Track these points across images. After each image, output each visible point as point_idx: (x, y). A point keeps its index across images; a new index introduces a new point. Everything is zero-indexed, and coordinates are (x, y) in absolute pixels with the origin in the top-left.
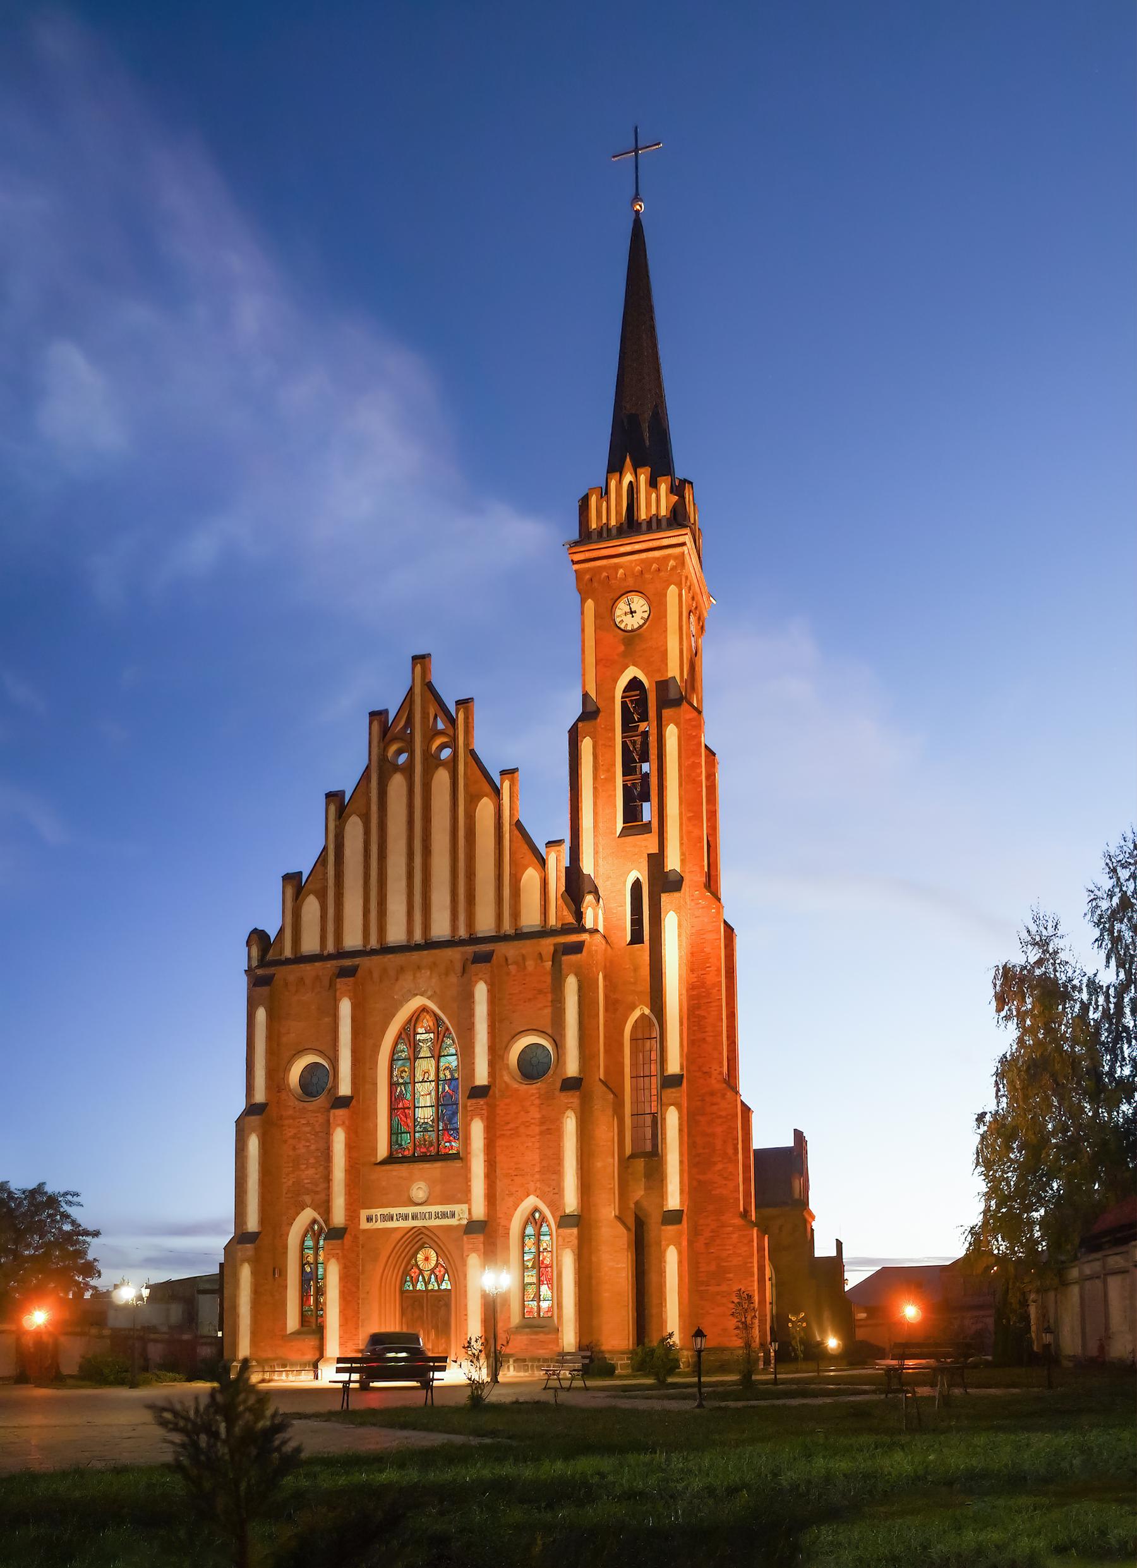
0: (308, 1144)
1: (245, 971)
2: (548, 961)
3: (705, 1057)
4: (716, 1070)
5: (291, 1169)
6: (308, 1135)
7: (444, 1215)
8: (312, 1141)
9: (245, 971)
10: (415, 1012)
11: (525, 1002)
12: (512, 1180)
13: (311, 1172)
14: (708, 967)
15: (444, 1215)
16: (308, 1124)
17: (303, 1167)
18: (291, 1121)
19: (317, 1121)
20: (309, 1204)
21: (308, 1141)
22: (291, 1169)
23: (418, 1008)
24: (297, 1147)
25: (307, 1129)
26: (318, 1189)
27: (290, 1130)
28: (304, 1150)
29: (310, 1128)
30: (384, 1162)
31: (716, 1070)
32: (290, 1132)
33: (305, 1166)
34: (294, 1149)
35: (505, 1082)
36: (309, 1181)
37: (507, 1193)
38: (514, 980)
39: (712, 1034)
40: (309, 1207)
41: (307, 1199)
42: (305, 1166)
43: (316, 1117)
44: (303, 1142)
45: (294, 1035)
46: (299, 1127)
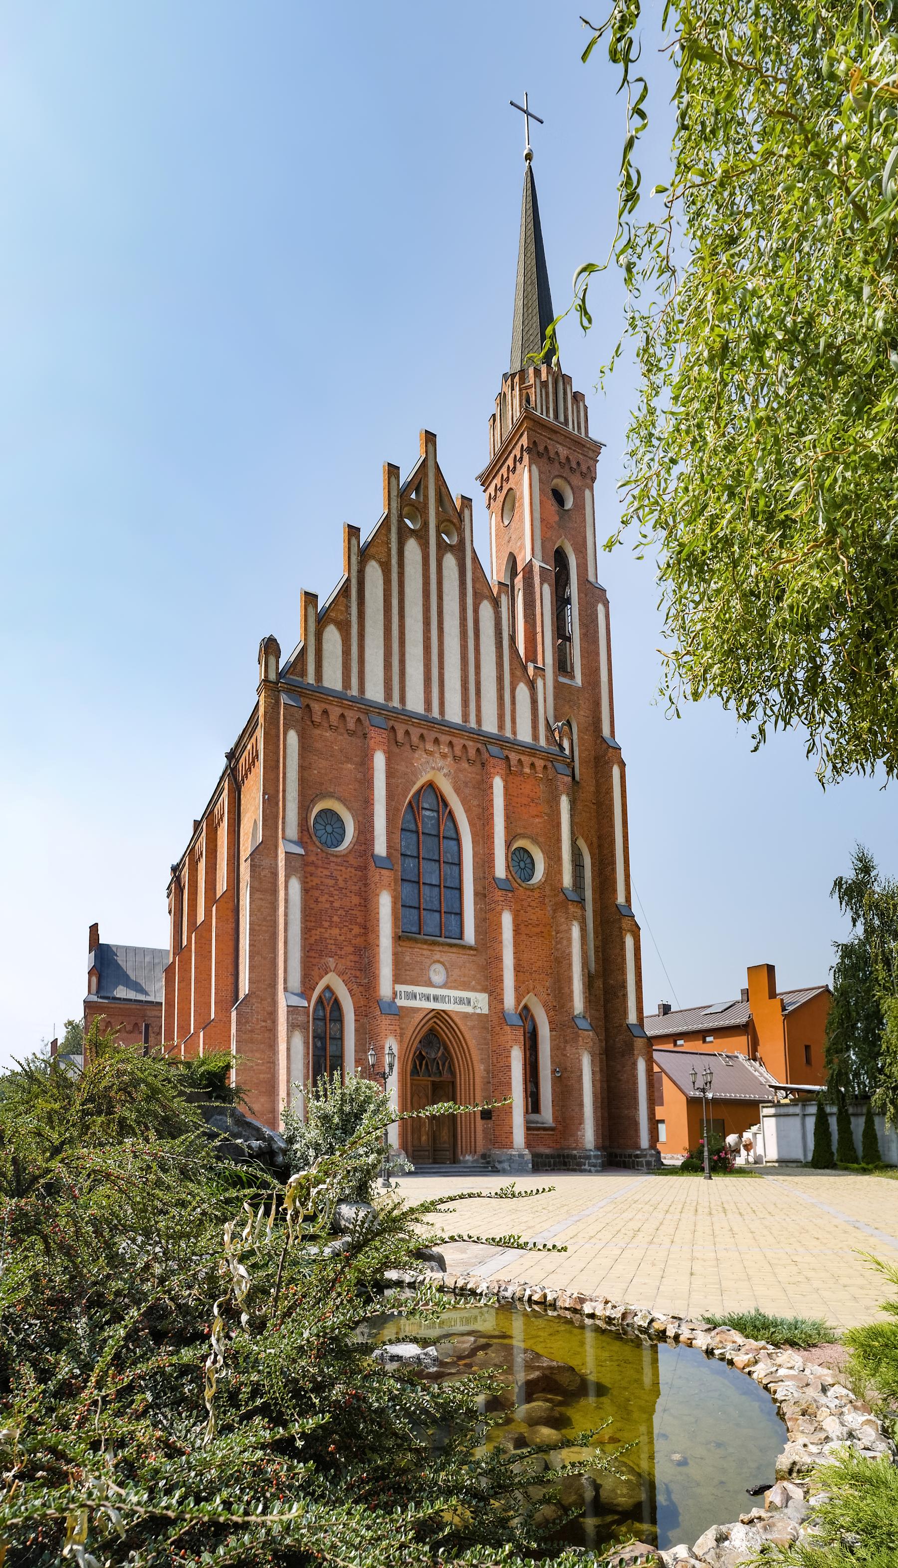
0: (331, 899)
5: (313, 924)
6: (332, 889)
7: (461, 1001)
8: (336, 897)
13: (336, 931)
15: (461, 1001)
16: (331, 876)
17: (326, 924)
18: (313, 868)
21: (332, 895)
22: (313, 924)
25: (331, 882)
26: (343, 953)
27: (313, 878)
28: (328, 906)
33: (328, 924)
34: (317, 901)
36: (333, 942)
41: (331, 962)
42: (328, 924)
44: (326, 896)
45: (316, 772)
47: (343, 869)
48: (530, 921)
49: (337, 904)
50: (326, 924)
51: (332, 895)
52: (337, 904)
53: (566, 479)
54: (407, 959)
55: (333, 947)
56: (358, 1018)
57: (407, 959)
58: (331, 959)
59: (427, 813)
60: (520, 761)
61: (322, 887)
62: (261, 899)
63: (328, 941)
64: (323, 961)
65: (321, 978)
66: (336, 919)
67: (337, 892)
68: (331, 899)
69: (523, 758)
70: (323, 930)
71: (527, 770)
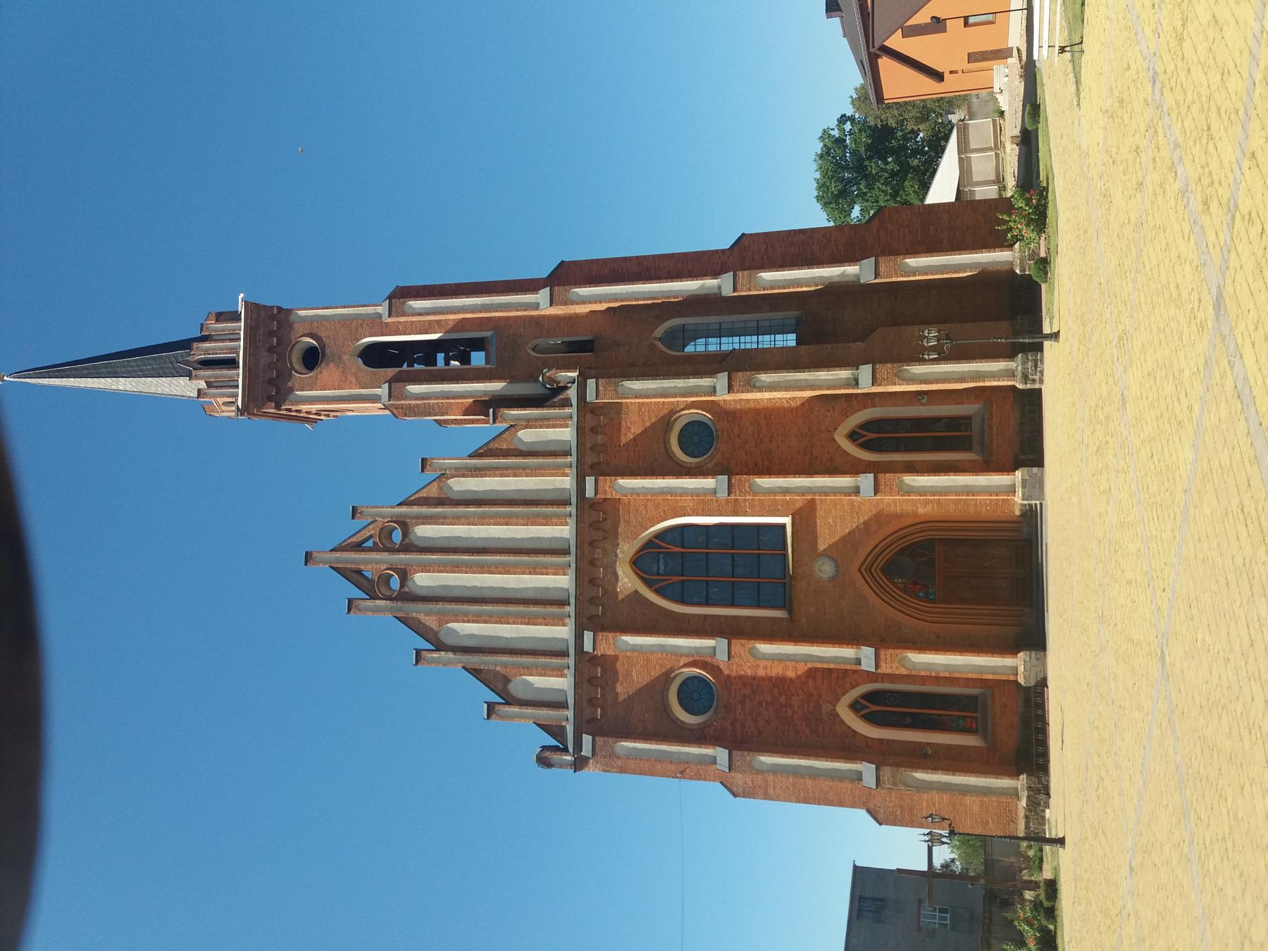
0: (764, 704)
1: (575, 771)
2: (600, 420)
3: (706, 270)
4: (720, 258)
5: (791, 728)
6: (754, 702)
9: (575, 771)
10: (637, 574)
11: (637, 446)
12: (816, 458)
14: (622, 270)
17: (790, 713)
19: (740, 690)
20: (833, 708)
23: (632, 569)
24: (767, 719)
25: (748, 702)
29: (747, 700)
30: (790, 612)
31: (720, 258)
32: (750, 727)
33: (788, 709)
34: (768, 722)
35: (714, 466)
36: (806, 705)
37: (829, 464)
38: (615, 457)
39: (685, 264)
40: (835, 706)
41: (826, 708)
42: (788, 709)
43: (735, 690)
45: (646, 715)
46: (745, 715)
47: (733, 687)
48: (756, 437)
49: (769, 698)
50: (790, 713)
51: (760, 703)
52: (769, 698)
53: (290, 351)
54: (812, 610)
55: (811, 704)
56: (880, 679)
57: (812, 610)
58: (823, 709)
59: (662, 567)
60: (591, 449)
61: (755, 714)
62: (774, 789)
63: (806, 710)
64: (826, 718)
65: (842, 722)
66: (783, 700)
67: (757, 696)
68: (764, 704)
69: (588, 445)
70: (796, 715)
71: (600, 437)
